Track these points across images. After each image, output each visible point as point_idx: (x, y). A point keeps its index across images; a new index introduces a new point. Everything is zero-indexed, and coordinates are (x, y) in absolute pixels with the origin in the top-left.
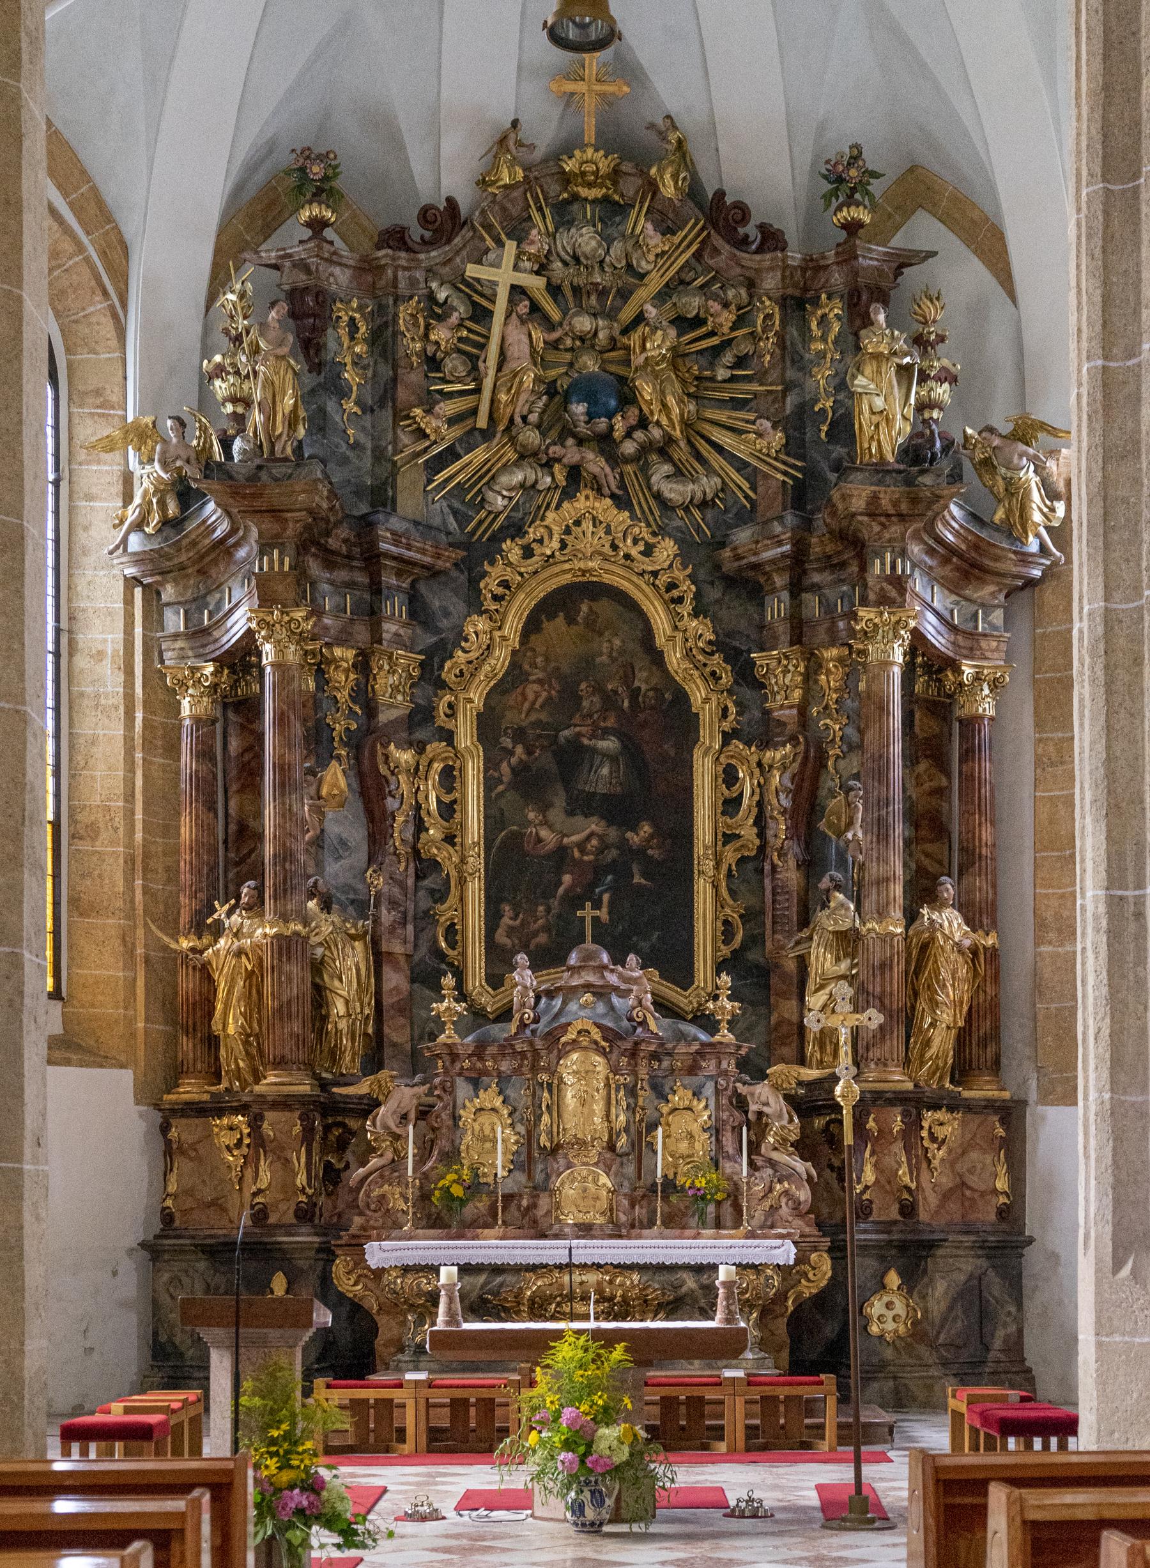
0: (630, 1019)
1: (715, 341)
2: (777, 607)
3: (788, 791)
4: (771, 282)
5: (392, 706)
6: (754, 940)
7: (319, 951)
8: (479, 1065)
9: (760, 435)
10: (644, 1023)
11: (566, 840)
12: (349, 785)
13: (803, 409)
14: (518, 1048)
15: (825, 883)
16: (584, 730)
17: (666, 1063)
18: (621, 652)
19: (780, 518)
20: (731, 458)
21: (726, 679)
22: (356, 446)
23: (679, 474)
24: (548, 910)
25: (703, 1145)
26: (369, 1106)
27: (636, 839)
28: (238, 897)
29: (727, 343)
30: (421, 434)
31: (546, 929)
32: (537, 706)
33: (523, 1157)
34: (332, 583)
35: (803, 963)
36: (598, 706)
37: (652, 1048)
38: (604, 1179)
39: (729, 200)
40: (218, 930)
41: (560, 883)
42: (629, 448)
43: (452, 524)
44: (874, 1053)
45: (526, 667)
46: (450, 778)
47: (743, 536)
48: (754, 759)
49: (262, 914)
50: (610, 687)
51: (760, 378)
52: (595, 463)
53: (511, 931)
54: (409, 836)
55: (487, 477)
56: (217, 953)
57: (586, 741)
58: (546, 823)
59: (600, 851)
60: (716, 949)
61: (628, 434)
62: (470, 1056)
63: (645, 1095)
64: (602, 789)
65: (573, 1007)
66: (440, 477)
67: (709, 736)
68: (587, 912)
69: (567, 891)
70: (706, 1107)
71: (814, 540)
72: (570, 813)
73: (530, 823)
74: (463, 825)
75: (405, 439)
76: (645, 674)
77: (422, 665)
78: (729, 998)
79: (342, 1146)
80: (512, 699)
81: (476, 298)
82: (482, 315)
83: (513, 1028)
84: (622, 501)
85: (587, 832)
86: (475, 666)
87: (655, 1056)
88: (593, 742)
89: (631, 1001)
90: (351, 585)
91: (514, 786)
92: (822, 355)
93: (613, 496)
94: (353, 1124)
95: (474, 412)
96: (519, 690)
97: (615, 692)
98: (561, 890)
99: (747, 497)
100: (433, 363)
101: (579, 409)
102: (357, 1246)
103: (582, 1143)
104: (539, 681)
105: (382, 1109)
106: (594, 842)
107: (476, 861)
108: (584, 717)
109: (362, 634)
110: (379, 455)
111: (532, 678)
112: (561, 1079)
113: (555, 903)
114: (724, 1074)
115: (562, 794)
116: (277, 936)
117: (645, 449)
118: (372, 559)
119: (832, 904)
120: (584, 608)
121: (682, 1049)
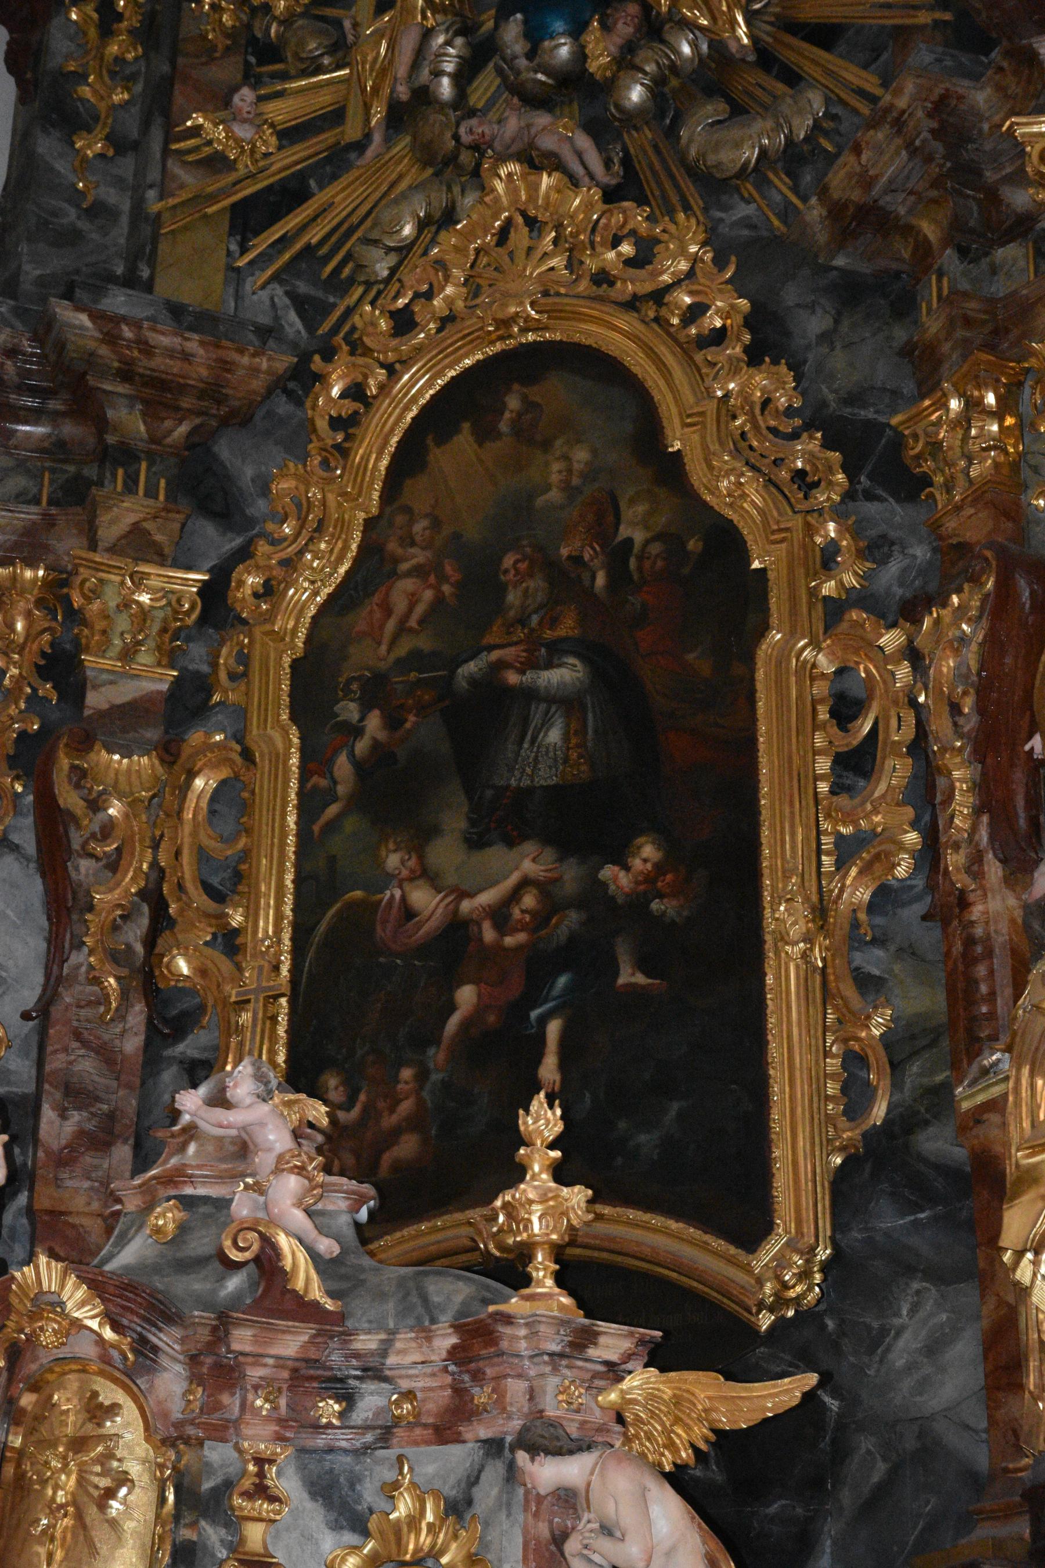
11: (466, 905)
16: (508, 653)
18: (590, 474)
24: (422, 1076)
27: (624, 880)
31: (415, 1123)
32: (413, 623)
36: (540, 597)
41: (451, 1007)
45: (393, 546)
50: (564, 552)
57: (513, 678)
58: (426, 874)
59: (541, 919)
64: (546, 776)
69: (466, 1025)
72: (476, 842)
73: (388, 879)
76: (641, 509)
80: (361, 620)
85: (514, 878)
88: (529, 676)
91: (358, 801)
96: (376, 598)
97: (577, 560)
98: (453, 1022)
104: (419, 571)
106: (529, 900)
108: (509, 627)
111: (404, 566)
113: (437, 1056)
115: (462, 798)
120: (513, 403)
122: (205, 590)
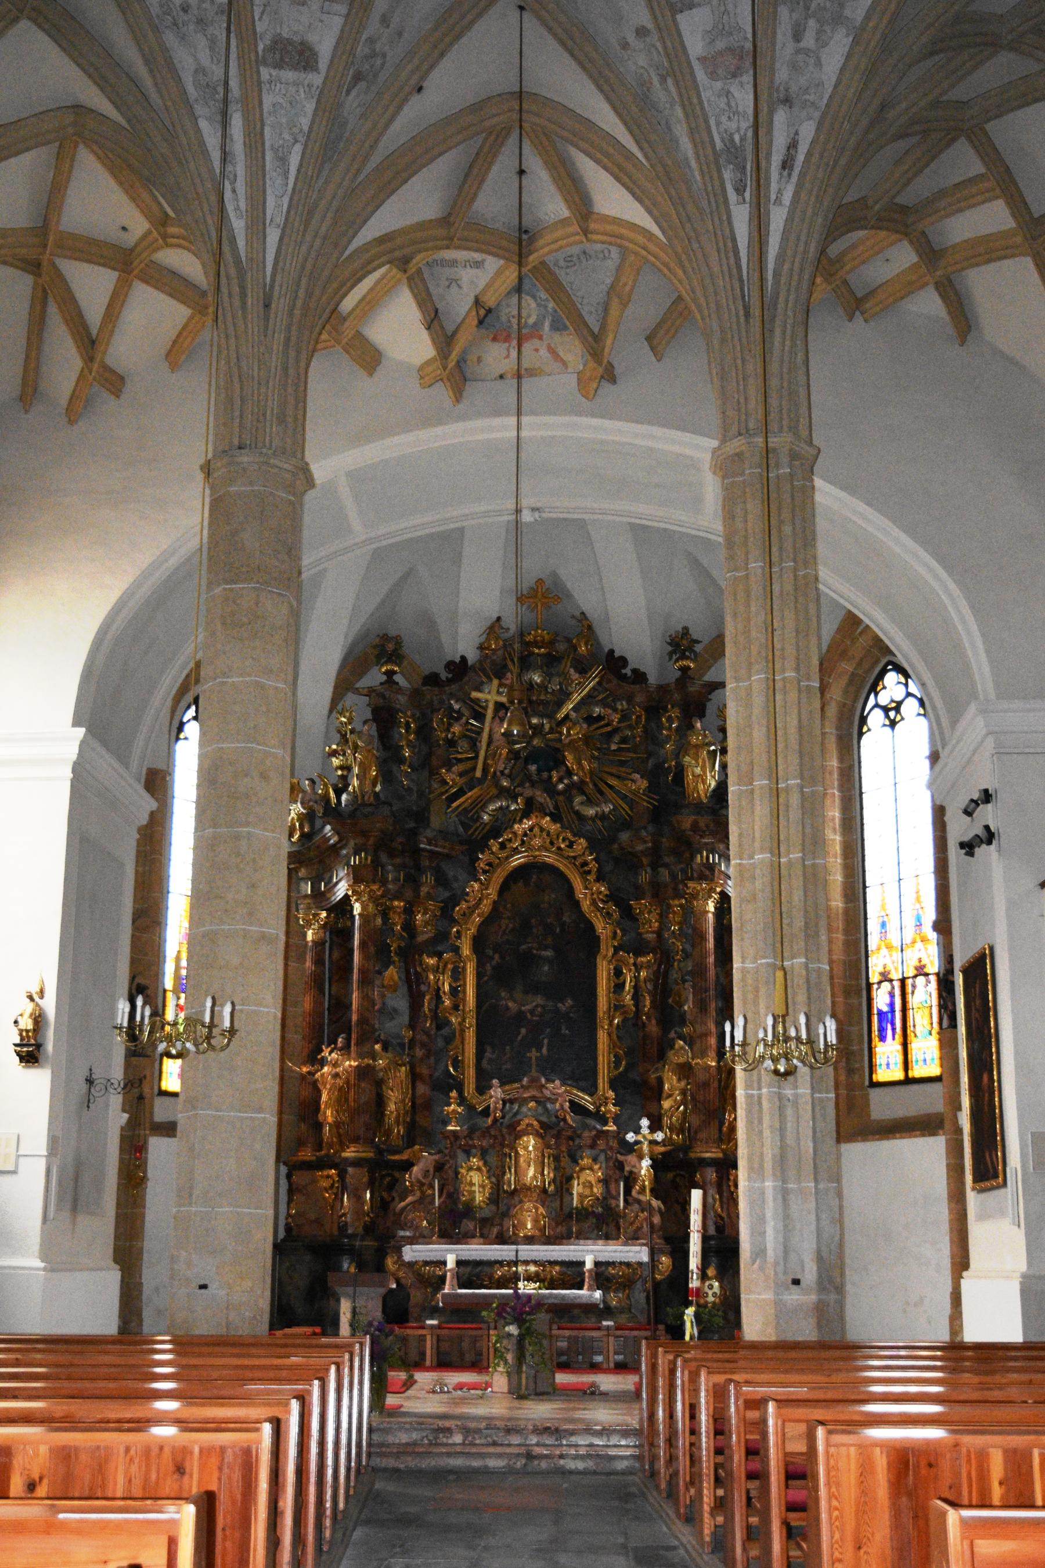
0: (557, 1117)
1: (609, 729)
2: (644, 877)
3: (650, 980)
4: (639, 698)
5: (426, 932)
6: (630, 1067)
7: (381, 1074)
8: (470, 1142)
9: (633, 781)
10: (564, 1120)
11: (523, 1008)
12: (400, 978)
13: (659, 766)
14: (493, 1133)
15: (672, 1035)
16: (535, 945)
17: (577, 1141)
19: (645, 828)
20: (618, 793)
21: (616, 915)
22: (409, 790)
23: (590, 802)
25: (598, 1190)
26: (408, 1166)
28: (335, 1043)
29: (616, 730)
30: (444, 782)
33: (495, 1197)
34: (393, 865)
35: (660, 1082)
37: (569, 1133)
38: (541, 1210)
39: (616, 655)
40: (323, 1062)
41: (519, 1033)
42: (561, 786)
43: (461, 829)
44: (700, 1136)
45: (501, 909)
46: (458, 974)
47: (624, 836)
48: (632, 961)
49: (349, 1053)
51: (634, 749)
52: (541, 797)
53: (490, 1060)
54: (433, 1006)
55: (480, 805)
56: (323, 1075)
59: (541, 1015)
60: (609, 1072)
61: (560, 780)
62: (465, 1138)
63: (565, 1161)
65: (524, 1109)
66: (455, 805)
67: (606, 950)
68: (533, 1054)
70: (600, 1168)
71: (664, 840)
72: (526, 992)
74: (464, 1000)
75: (435, 785)
77: (442, 909)
78: (614, 1105)
79: (391, 1187)
81: (477, 708)
82: (480, 717)
83: (490, 1121)
84: (555, 818)
85: (534, 1004)
86: (472, 910)
87: (571, 1138)
89: (558, 1106)
90: (404, 866)
92: (669, 737)
93: (551, 815)
94: (397, 1175)
95: (474, 769)
98: (519, 1038)
99: (627, 813)
100: (451, 743)
101: (533, 768)
102: (398, 1250)
103: (529, 1189)
104: (508, 918)
105: (415, 1169)
107: (471, 1021)
109: (409, 894)
110: (421, 794)
112: (517, 1153)
114: (611, 1148)
116: (357, 1067)
117: (569, 788)
118: (416, 852)
119: (677, 1046)
121: (586, 1134)
122: (442, 909)
